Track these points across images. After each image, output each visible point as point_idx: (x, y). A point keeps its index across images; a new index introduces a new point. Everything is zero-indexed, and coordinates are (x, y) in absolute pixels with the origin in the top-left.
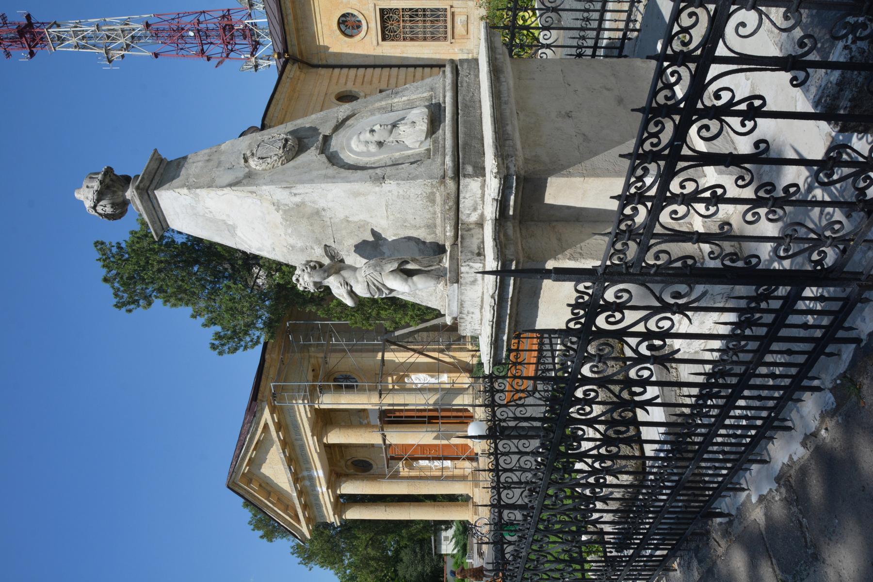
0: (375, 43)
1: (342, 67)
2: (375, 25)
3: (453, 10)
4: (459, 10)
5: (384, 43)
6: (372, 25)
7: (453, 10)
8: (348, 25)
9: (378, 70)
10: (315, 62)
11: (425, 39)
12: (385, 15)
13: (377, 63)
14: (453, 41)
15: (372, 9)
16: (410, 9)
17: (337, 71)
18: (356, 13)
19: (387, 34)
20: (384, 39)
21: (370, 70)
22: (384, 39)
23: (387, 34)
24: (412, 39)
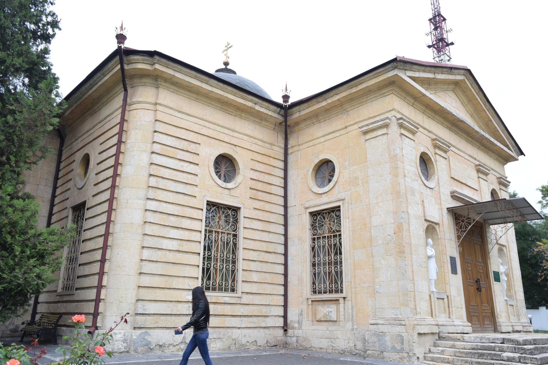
0: (307, 205)
1: (286, 170)
2: (324, 202)
3: (341, 301)
4: (342, 309)
5: (308, 214)
6: (325, 199)
7: (341, 301)
8: (325, 170)
9: (281, 210)
10: (291, 143)
11: (314, 265)
12: (334, 212)
13: (289, 210)
14: (310, 302)
15: (341, 196)
16: (341, 244)
17: (281, 165)
18: (335, 179)
19: (317, 216)
20: (313, 215)
21: (281, 201)
22: (313, 215)
23: (317, 216)
24: (313, 248)
